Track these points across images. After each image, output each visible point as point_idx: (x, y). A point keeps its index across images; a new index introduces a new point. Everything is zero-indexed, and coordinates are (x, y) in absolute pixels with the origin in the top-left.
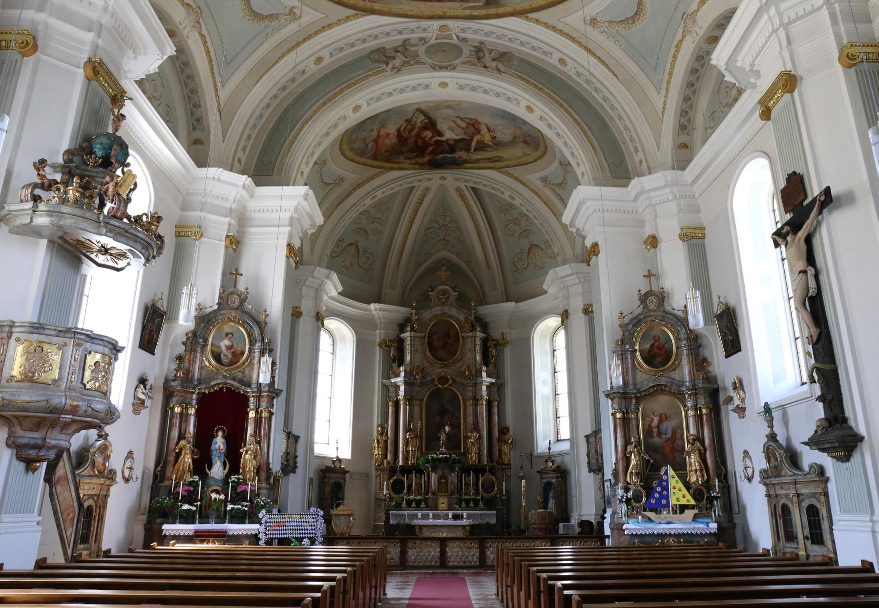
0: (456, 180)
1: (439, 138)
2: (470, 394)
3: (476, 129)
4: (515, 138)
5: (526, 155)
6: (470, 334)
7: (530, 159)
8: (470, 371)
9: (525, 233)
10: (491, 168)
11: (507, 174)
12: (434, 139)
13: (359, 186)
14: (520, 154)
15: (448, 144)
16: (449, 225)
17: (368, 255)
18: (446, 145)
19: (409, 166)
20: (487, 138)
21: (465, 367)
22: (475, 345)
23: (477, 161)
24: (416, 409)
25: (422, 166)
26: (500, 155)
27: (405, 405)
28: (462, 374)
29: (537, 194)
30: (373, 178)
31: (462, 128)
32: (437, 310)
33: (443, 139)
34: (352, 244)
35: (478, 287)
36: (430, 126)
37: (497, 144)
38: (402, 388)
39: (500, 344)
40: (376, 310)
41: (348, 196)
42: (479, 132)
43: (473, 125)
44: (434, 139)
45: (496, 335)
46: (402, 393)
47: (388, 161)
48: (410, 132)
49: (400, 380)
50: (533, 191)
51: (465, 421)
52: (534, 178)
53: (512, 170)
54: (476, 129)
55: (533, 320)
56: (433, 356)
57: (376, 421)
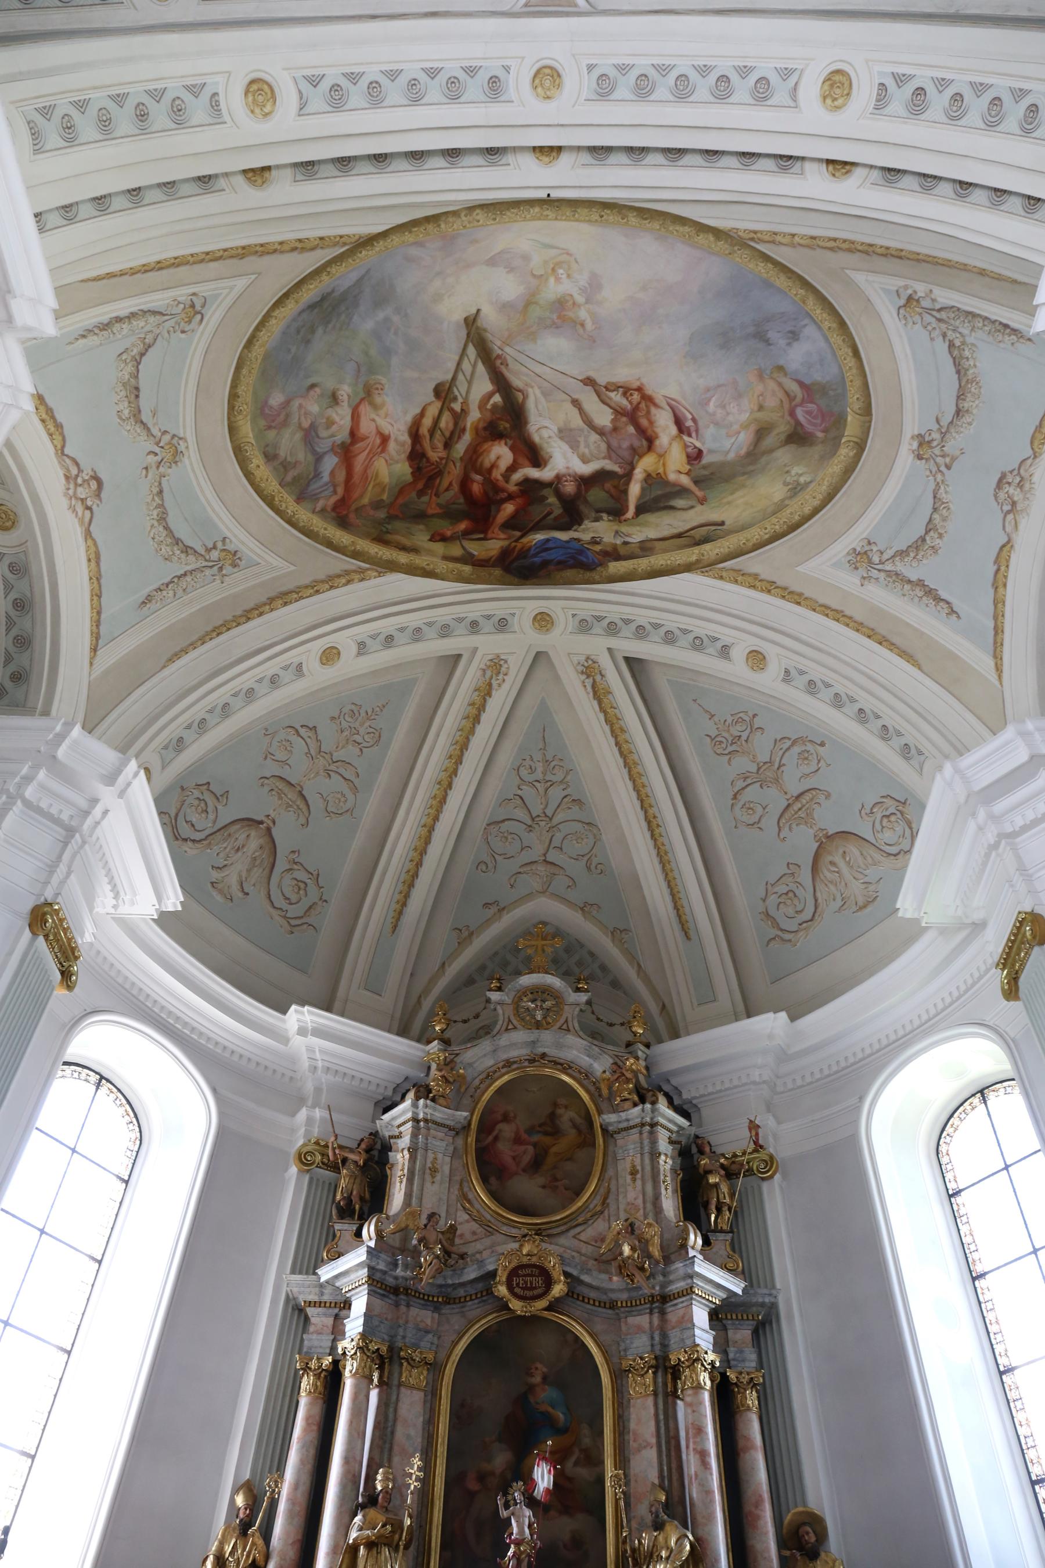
0: (584, 626)
1: (534, 473)
2: (639, 1346)
3: (641, 431)
4: (761, 432)
5: (796, 489)
6: (635, 1113)
7: (807, 501)
8: (642, 1245)
9: (798, 806)
10: (688, 568)
11: (739, 577)
12: (517, 476)
13: (285, 597)
14: (778, 492)
15: (558, 494)
16: (559, 817)
17: (302, 875)
18: (552, 500)
19: (442, 566)
20: (674, 464)
21: (618, 1225)
22: (655, 1155)
23: (646, 548)
24: (411, 1405)
25: (481, 570)
26: (715, 516)
27: (364, 1378)
28: (610, 1260)
29: (838, 615)
30: (331, 582)
31: (601, 432)
32: (515, 1043)
33: (545, 474)
34: (251, 822)
35: (654, 1008)
36: (504, 425)
37: (709, 477)
38: (359, 1305)
39: (751, 1167)
40: (302, 1032)
41: (247, 616)
42: (650, 441)
43: (632, 416)
44: (517, 476)
45: (729, 1139)
46: (354, 1325)
47: (380, 540)
48: (448, 445)
49: (349, 1267)
50: (826, 610)
51: (622, 1461)
52: (822, 560)
53: (751, 563)
54: (641, 431)
55: (852, 1079)
56: (493, 1195)
57: (235, 1461)
